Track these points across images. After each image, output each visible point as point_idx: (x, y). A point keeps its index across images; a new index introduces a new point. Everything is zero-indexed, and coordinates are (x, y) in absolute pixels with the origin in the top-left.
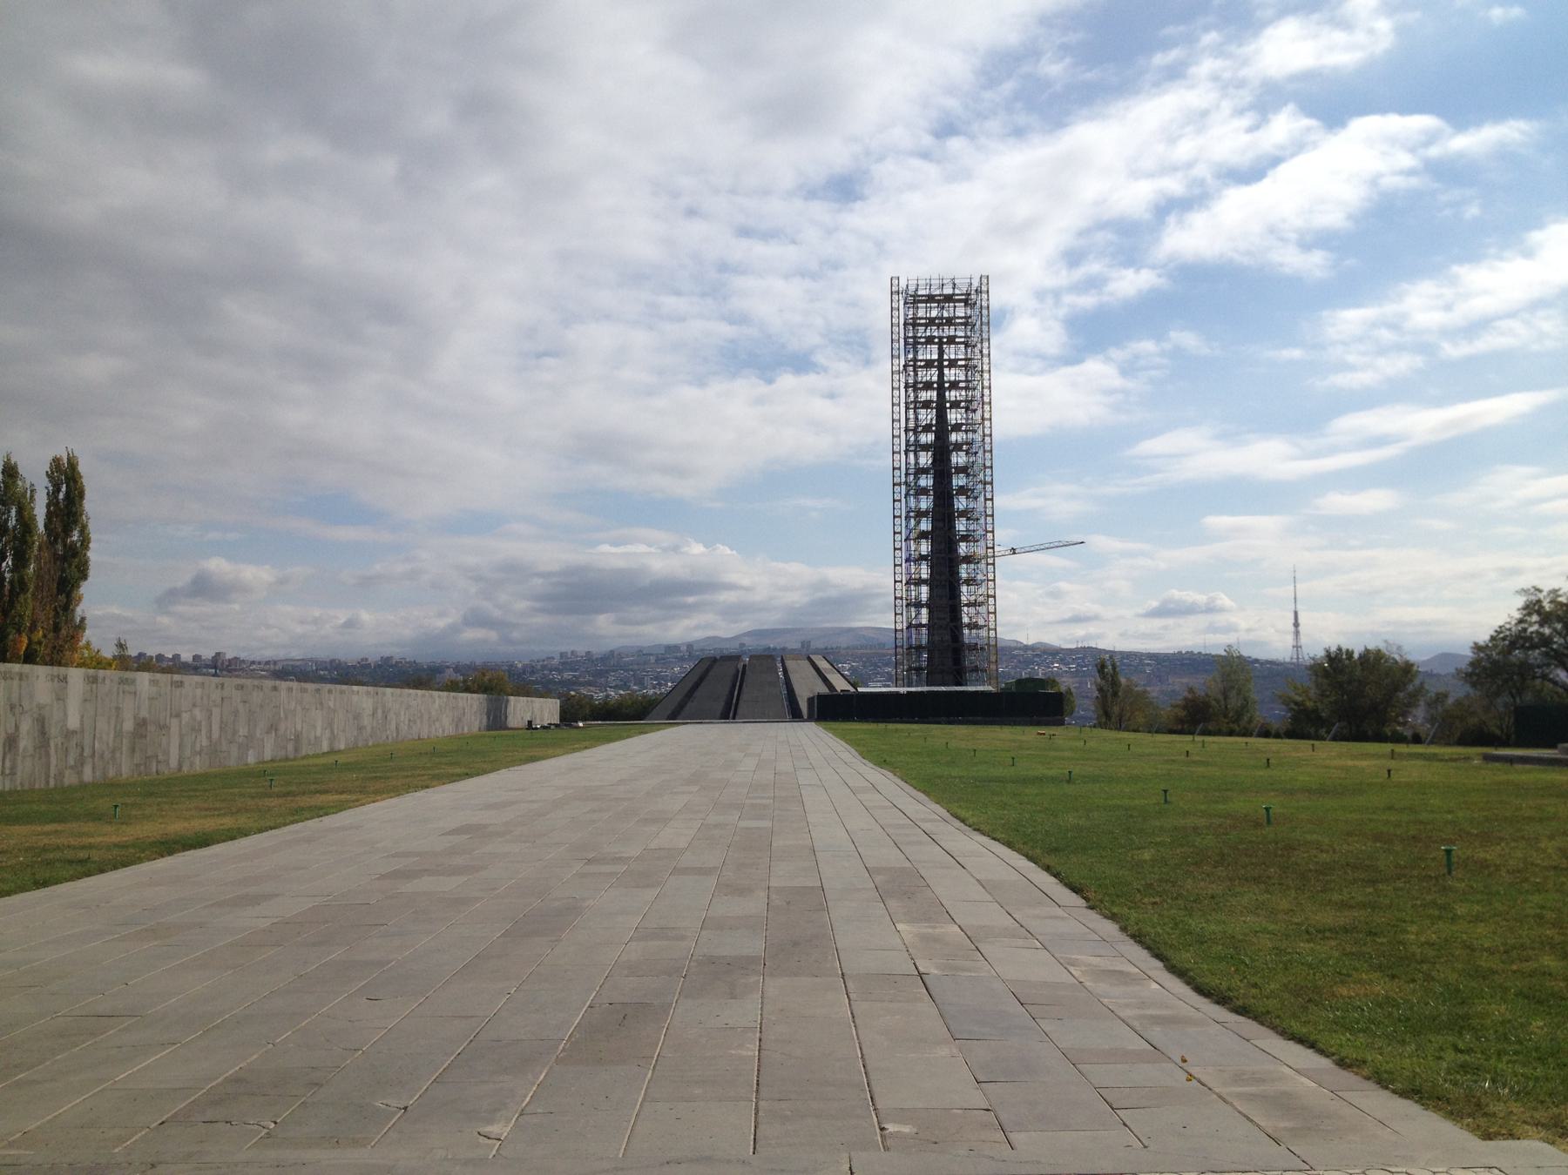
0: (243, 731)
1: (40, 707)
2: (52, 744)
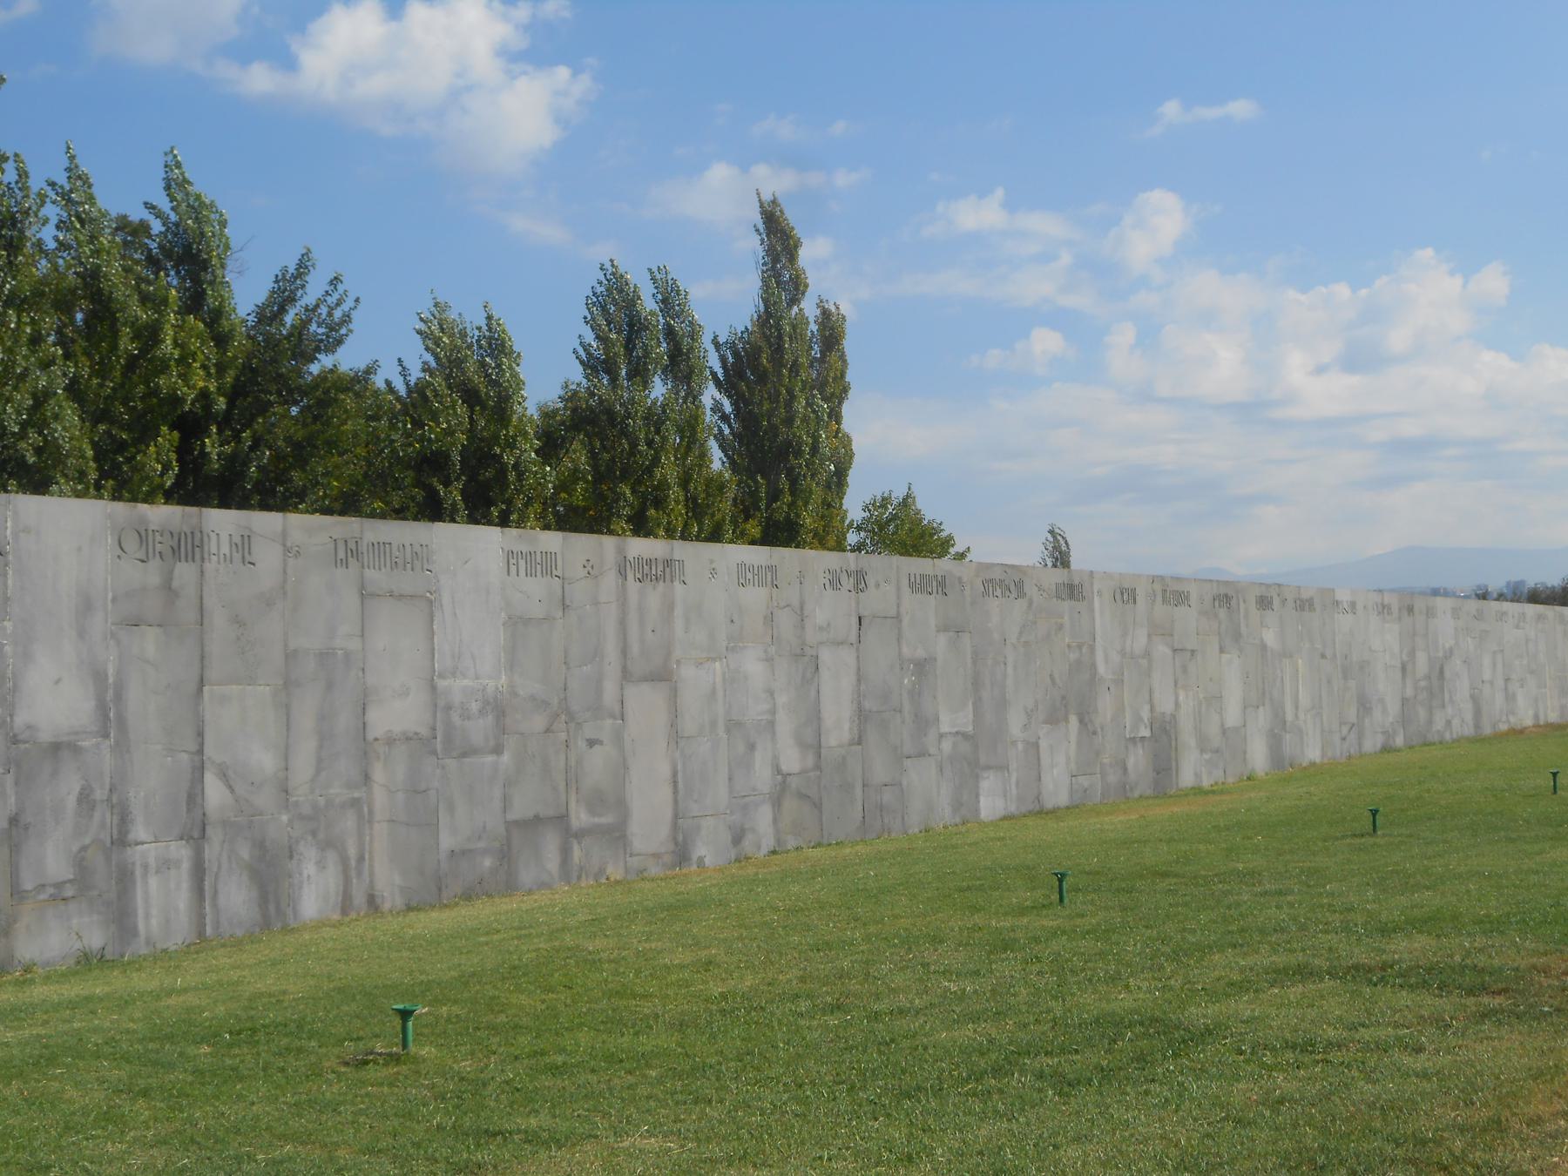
0: (952, 719)
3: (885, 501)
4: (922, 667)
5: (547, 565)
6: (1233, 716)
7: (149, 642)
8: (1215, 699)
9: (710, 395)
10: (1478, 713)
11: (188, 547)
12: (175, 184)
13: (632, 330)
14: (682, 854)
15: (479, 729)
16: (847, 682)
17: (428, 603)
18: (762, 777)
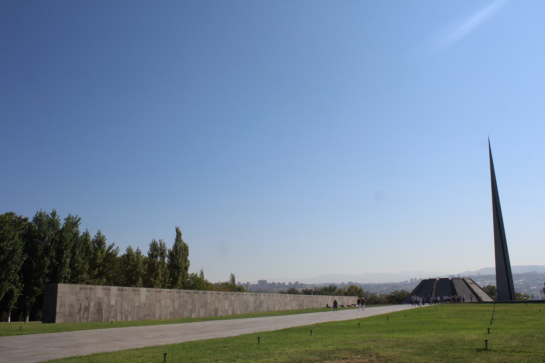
0: (189, 307)
1: (98, 298)
2: (104, 310)
3: (193, 274)
4: (186, 301)
5: (149, 291)
6: (226, 308)
7: (119, 298)
8: (224, 306)
9: (166, 259)
10: (268, 309)
11: (122, 290)
12: (99, 234)
13: (156, 249)
14: (160, 318)
15: (143, 306)
16: (178, 303)
17: (140, 295)
18: (168, 312)
